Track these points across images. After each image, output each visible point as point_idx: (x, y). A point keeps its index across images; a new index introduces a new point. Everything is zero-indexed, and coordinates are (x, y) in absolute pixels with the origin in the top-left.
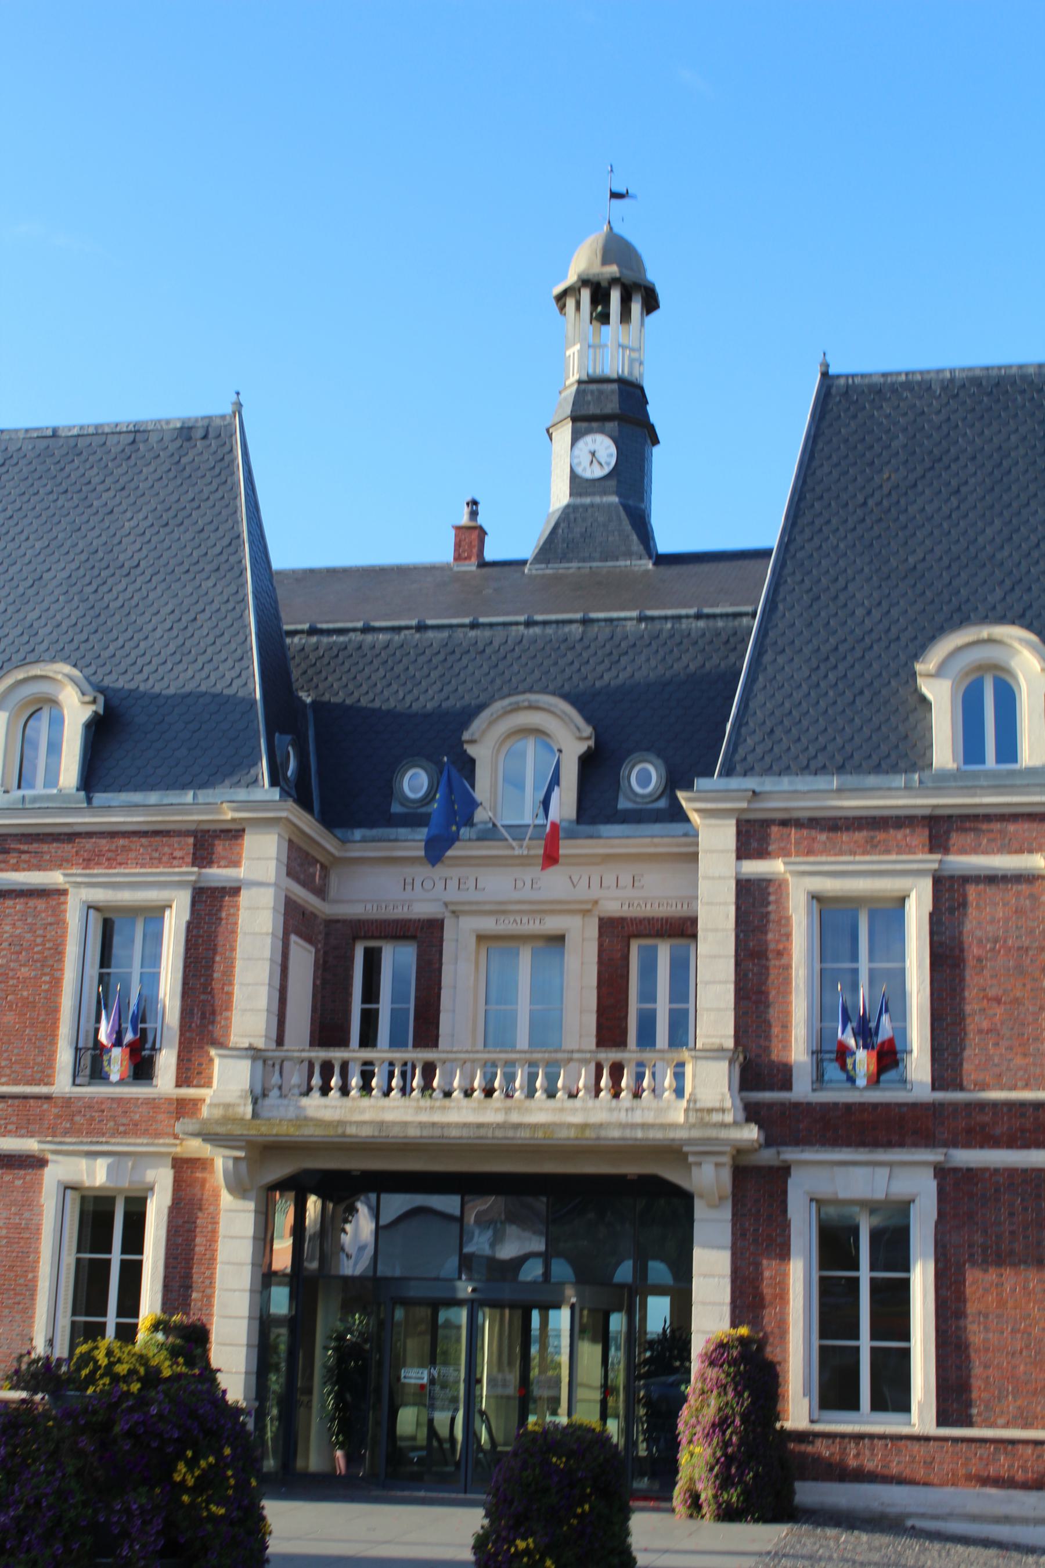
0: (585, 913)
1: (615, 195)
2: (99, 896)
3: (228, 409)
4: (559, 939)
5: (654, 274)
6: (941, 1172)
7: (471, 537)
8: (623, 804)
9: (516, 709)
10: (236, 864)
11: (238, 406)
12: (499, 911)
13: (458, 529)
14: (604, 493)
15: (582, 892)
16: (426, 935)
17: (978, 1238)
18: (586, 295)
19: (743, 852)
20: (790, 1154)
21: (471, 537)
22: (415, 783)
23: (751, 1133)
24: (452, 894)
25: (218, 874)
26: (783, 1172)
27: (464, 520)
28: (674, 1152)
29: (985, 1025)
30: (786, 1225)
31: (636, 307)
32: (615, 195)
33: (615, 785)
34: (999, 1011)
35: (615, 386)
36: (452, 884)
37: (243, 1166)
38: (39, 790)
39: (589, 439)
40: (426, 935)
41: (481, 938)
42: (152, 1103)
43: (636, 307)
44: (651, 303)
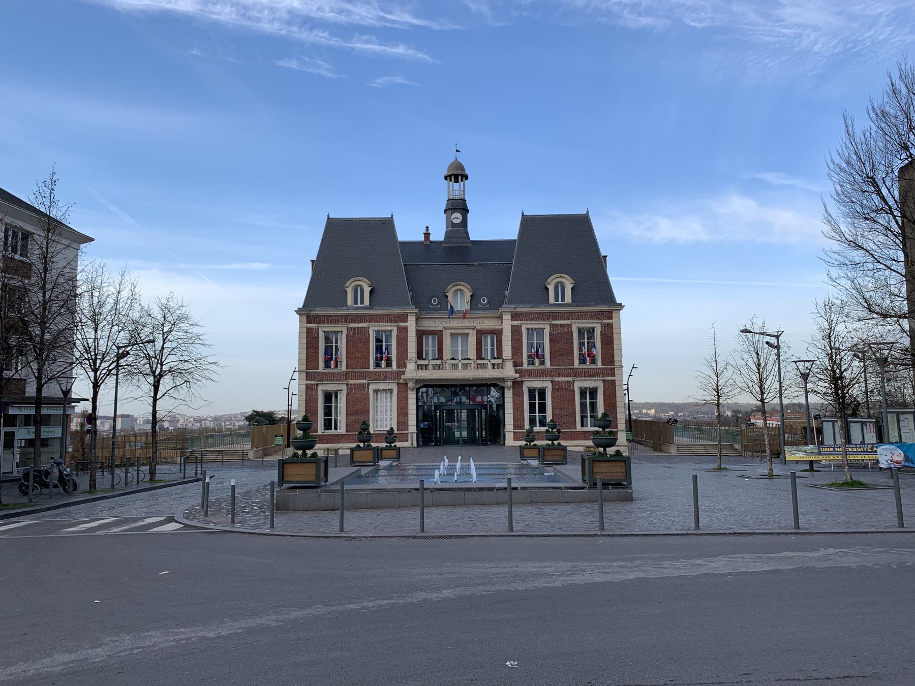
2: (377, 329)
5: (467, 172)
6: (552, 382)
7: (427, 235)
10: (406, 322)
15: (472, 325)
16: (439, 334)
21: (427, 235)
22: (435, 301)
23: (518, 375)
24: (445, 325)
25: (402, 324)
26: (523, 382)
28: (503, 380)
38: (359, 305)
40: (439, 334)
42: (392, 372)
44: (467, 177)
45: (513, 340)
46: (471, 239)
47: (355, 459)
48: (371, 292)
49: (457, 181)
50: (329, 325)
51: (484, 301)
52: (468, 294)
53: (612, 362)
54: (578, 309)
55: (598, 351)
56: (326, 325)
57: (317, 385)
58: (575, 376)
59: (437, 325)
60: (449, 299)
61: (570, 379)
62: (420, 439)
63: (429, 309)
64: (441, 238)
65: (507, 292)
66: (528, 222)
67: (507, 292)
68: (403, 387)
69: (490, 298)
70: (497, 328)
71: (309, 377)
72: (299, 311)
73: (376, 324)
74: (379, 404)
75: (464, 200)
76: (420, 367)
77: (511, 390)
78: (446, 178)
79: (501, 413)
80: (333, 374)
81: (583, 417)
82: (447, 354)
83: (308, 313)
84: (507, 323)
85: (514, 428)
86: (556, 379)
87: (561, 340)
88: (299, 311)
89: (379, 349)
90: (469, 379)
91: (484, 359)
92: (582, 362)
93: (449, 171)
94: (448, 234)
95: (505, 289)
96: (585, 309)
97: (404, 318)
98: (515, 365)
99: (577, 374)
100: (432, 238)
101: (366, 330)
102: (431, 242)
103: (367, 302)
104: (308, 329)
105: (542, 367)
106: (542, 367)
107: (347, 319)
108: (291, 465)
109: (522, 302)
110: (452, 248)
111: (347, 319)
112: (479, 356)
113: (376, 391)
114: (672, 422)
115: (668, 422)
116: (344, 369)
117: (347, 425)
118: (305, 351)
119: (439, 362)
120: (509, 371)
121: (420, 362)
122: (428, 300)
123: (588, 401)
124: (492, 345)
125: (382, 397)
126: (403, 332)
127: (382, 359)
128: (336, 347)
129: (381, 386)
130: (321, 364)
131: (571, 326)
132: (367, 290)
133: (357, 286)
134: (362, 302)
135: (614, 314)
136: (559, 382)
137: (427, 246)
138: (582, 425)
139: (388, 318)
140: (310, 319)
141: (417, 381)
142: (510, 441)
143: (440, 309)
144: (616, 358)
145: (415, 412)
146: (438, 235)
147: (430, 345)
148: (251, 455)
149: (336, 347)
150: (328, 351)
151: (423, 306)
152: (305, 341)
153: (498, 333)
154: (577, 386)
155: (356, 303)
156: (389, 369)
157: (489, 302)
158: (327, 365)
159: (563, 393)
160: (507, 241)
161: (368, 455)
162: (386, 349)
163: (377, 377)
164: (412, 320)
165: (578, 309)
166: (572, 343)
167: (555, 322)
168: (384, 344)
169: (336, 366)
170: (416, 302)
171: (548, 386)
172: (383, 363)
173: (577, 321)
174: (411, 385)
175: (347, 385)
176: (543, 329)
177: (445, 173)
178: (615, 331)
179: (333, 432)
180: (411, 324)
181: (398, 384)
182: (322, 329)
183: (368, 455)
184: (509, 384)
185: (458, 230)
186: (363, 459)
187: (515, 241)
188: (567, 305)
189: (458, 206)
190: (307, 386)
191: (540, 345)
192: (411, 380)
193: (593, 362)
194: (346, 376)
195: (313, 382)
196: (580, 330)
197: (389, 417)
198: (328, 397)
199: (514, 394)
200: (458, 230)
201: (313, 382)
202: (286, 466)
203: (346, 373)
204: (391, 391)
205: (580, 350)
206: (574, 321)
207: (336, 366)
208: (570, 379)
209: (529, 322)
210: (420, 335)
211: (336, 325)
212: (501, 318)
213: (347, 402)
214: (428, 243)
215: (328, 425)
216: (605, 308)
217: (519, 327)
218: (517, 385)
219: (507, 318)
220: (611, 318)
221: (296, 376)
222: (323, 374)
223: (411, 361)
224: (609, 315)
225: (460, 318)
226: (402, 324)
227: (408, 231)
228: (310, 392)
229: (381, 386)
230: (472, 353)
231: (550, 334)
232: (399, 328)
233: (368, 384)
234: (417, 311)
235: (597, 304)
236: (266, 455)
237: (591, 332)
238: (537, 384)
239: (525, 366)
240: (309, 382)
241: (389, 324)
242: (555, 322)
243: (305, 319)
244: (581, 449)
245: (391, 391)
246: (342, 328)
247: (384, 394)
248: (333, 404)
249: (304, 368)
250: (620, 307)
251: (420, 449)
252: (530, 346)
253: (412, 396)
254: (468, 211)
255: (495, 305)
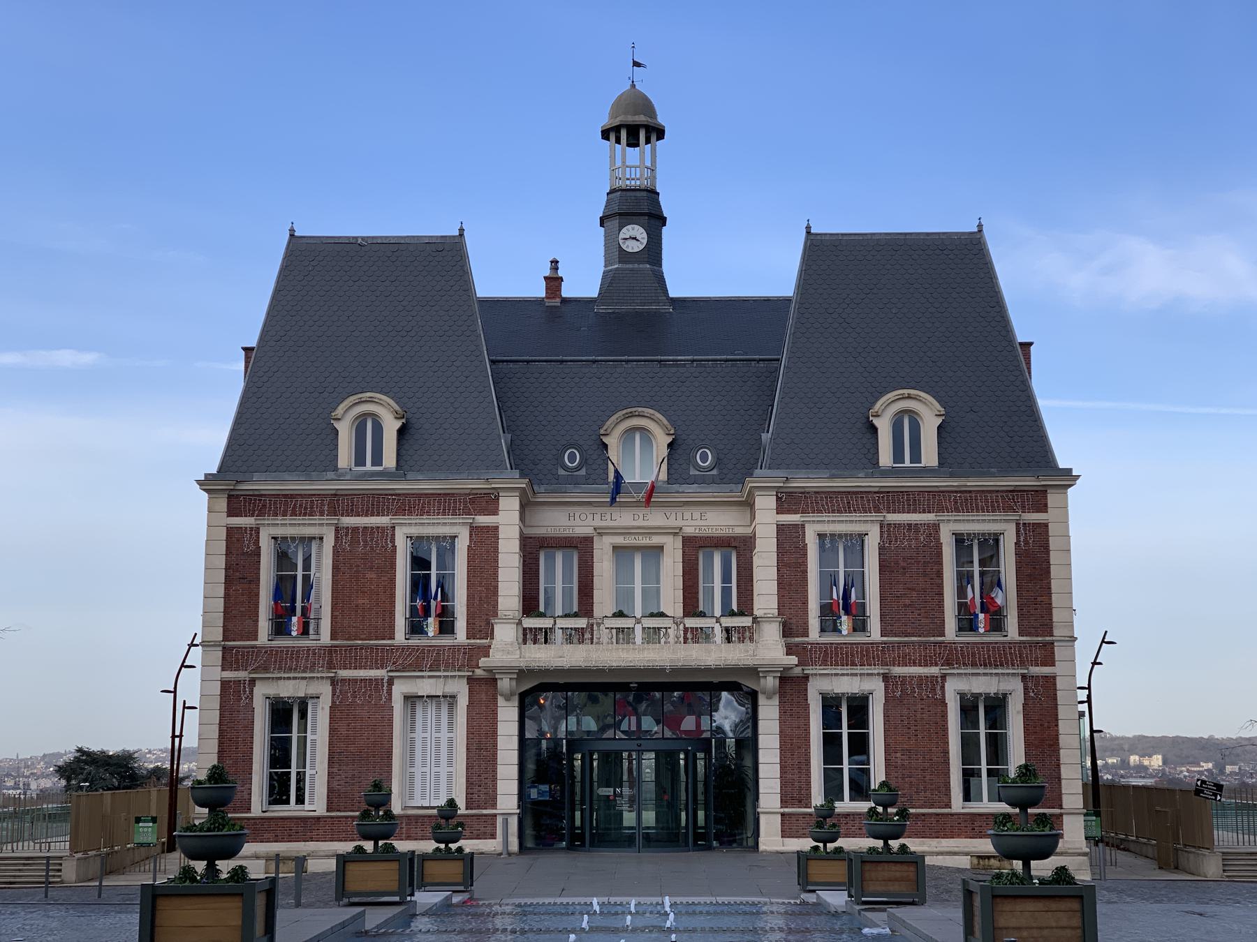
0: (675, 534)
1: (636, 64)
2: (415, 531)
3: (457, 233)
4: (660, 548)
5: (661, 119)
6: (886, 678)
7: (554, 282)
8: (693, 472)
9: (632, 415)
10: (495, 512)
11: (462, 230)
12: (626, 531)
13: (546, 278)
14: (640, 262)
16: (582, 547)
17: (905, 712)
18: (624, 134)
19: (780, 511)
20: (809, 670)
21: (554, 282)
23: (793, 660)
24: (598, 522)
25: (483, 520)
27: (547, 274)
28: (753, 672)
29: (908, 602)
30: (807, 706)
31: (654, 137)
32: (636, 64)
33: (691, 461)
34: (914, 594)
35: (645, 194)
36: (597, 517)
37: (514, 683)
38: (369, 466)
39: (629, 227)
40: (582, 547)
41: (616, 548)
42: (455, 649)
43: (654, 137)
44: (661, 134)
45: (781, 565)
46: (673, 293)
47: (351, 886)
48: (402, 432)
49: (633, 143)
50: (288, 520)
51: (705, 459)
52: (662, 441)
53: (1048, 628)
54: (954, 483)
55: (1008, 597)
56: (279, 520)
57: (253, 682)
58: (948, 663)
59: (577, 523)
60: (613, 454)
61: (934, 670)
62: (529, 832)
63: (557, 477)
64: (592, 291)
65: (764, 436)
66: (822, 253)
67: (766, 437)
68: (484, 688)
69: (718, 453)
70: (739, 531)
71: (230, 659)
72: (207, 483)
73: (414, 519)
74: (419, 735)
75: (653, 193)
76: (530, 636)
77: (776, 701)
78: (605, 134)
79: (748, 762)
80: (295, 653)
81: (969, 775)
82: (604, 601)
83: (232, 487)
84: (766, 520)
85: (784, 803)
86: (898, 670)
87: (909, 566)
88: (207, 483)
89: (419, 586)
90: (662, 670)
91: (702, 615)
92: (967, 623)
93: (614, 114)
94: (610, 282)
95: (763, 425)
96: (973, 483)
97: (488, 503)
98: (787, 631)
99: (952, 657)
100: (567, 292)
101: (388, 534)
102: (565, 301)
103: (389, 460)
104: (231, 531)
105: (859, 638)
106: (859, 638)
107: (336, 504)
108: (176, 902)
109: (808, 464)
110: (618, 317)
111: (336, 504)
112: (691, 608)
113: (411, 700)
114: (1208, 790)
115: (1198, 792)
116: (325, 638)
117: (330, 791)
118: (221, 591)
119: (581, 623)
120: (770, 648)
121: (530, 623)
122: (553, 454)
123: (982, 731)
124: (726, 578)
125: (426, 715)
126: (485, 541)
127: (427, 612)
128: (306, 578)
129: (425, 686)
130: (264, 626)
131: (936, 527)
132: (391, 427)
133: (363, 417)
134: (377, 460)
135: (1052, 499)
136: (904, 679)
137: (554, 309)
138: (967, 797)
139: (447, 503)
140: (237, 504)
141: (522, 674)
142: (771, 837)
143: (587, 480)
144: (1057, 616)
145: (514, 757)
146: (584, 283)
147: (558, 577)
148: (69, 872)
149: (306, 578)
150: (284, 589)
151: (539, 474)
152: (221, 562)
153: (743, 546)
154: (953, 689)
155: (360, 460)
156: (446, 641)
157: (718, 463)
158: (280, 628)
159: (915, 708)
160: (767, 300)
161: (386, 875)
162: (440, 585)
163: (417, 661)
164: (509, 507)
165: (954, 483)
166: (940, 574)
167: (893, 518)
168: (434, 572)
169: (305, 632)
170: (521, 460)
171: (875, 688)
172: (432, 625)
173: (953, 516)
174: (505, 684)
175: (334, 682)
176: (862, 537)
177: (604, 121)
178: (1053, 543)
179: (291, 809)
180: (507, 519)
181: (470, 680)
182: (269, 531)
183: (386, 875)
184: (771, 682)
185: (637, 272)
186: (371, 886)
187: (788, 300)
188: (927, 472)
189: (637, 208)
190: (225, 684)
191: (855, 580)
192: (506, 670)
193: (997, 624)
194: (331, 658)
195: (242, 675)
196: (961, 541)
197: (444, 770)
198: (282, 714)
199: (783, 712)
200: (637, 272)
201: (242, 675)
202: (162, 904)
203: (331, 650)
204: (451, 699)
205: (961, 592)
206: (945, 516)
207: (305, 632)
208: (934, 670)
209: (825, 517)
210: (532, 548)
211: (307, 520)
212: (749, 504)
213: (333, 731)
214: (557, 302)
215: (278, 791)
216: (1028, 482)
217: (799, 529)
218: (791, 687)
219: (766, 503)
220: (1043, 508)
221: (196, 656)
222: (270, 651)
223: (507, 620)
224: (1038, 500)
225: (637, 504)
226: (483, 520)
227: (504, 271)
228: (232, 701)
229: (425, 686)
230: (671, 599)
231: (882, 549)
232: (475, 530)
233: (391, 682)
234: (523, 484)
235: (1005, 472)
236: (108, 871)
237: (991, 544)
238: (846, 684)
239: (814, 635)
240: (229, 675)
241: (449, 519)
242: (893, 518)
243: (222, 504)
244: (964, 862)
245: (451, 699)
246: (323, 529)
247: (431, 709)
248: (295, 735)
249: (218, 634)
250: (1068, 478)
251: (526, 859)
252: (829, 581)
253: (508, 716)
254: (663, 221)
255: (735, 471)
